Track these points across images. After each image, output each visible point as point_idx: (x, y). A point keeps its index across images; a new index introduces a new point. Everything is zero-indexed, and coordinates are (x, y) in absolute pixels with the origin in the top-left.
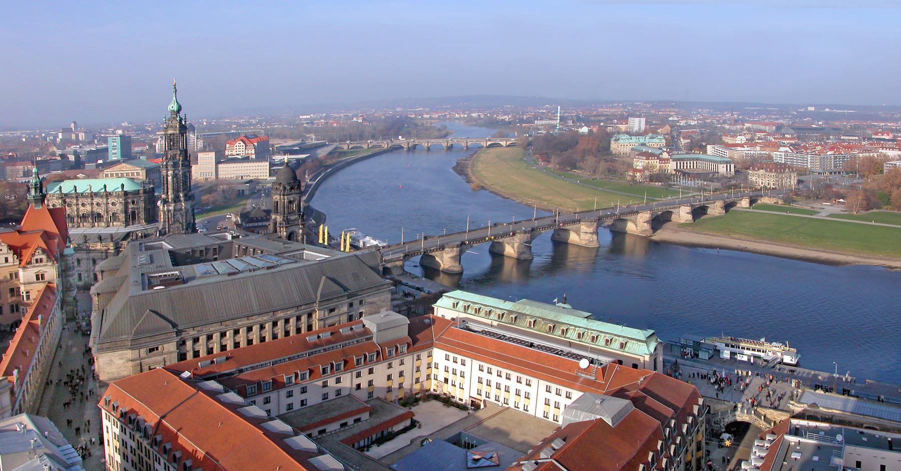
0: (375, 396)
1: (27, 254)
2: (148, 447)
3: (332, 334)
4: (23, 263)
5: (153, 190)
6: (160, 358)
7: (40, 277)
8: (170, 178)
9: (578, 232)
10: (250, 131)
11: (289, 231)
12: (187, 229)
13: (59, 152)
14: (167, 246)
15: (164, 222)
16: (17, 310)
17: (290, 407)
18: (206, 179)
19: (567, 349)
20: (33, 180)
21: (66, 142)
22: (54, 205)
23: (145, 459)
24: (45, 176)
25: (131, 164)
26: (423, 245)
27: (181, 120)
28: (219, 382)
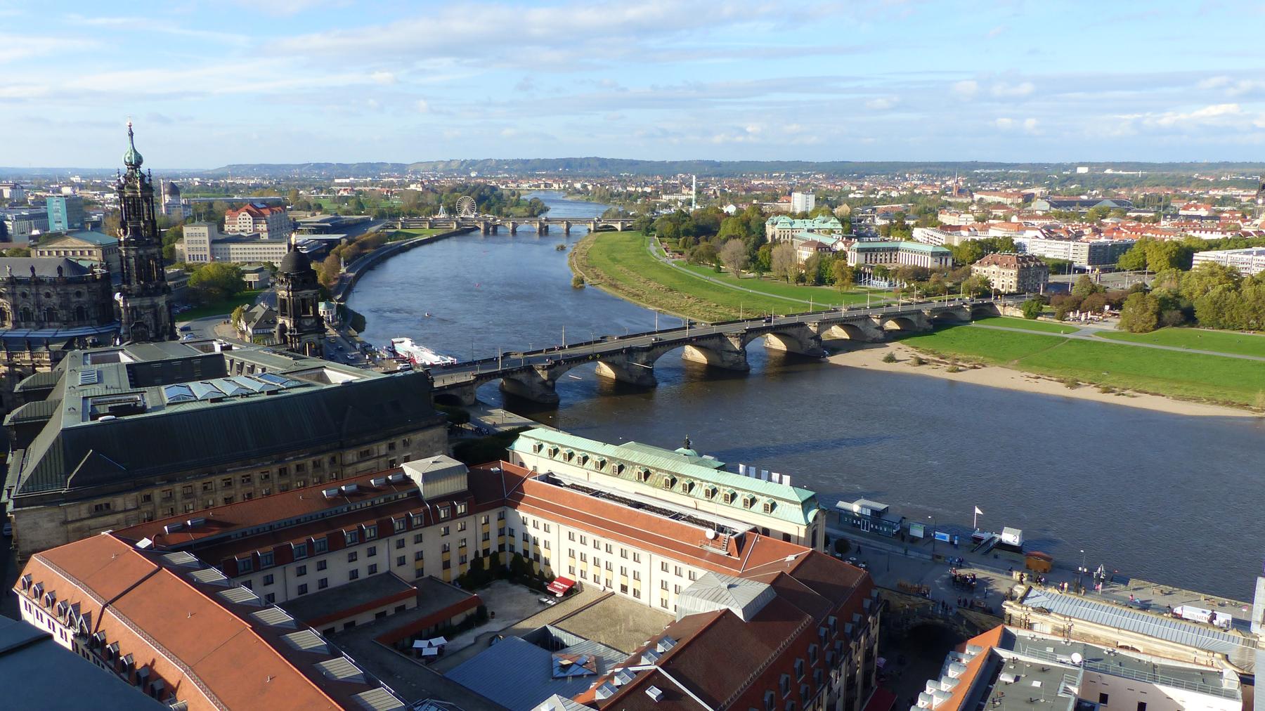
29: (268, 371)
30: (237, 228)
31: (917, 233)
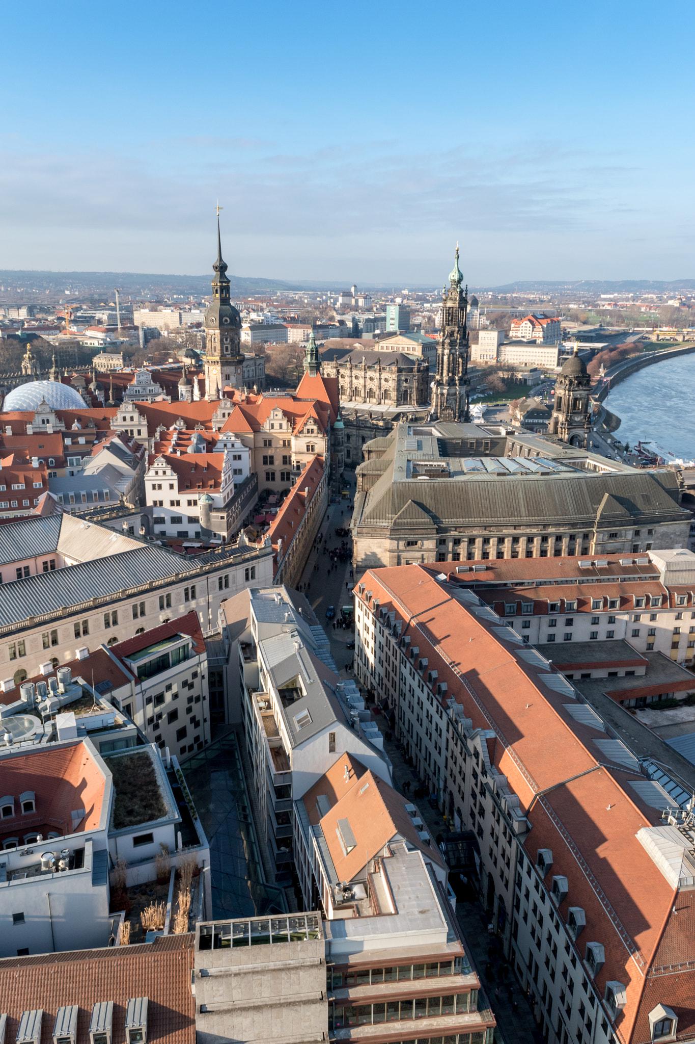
0: (655, 650)
1: (300, 422)
2: (396, 647)
3: (609, 563)
4: (296, 431)
5: (427, 369)
6: (419, 554)
7: (310, 448)
8: (446, 358)
10: (539, 309)
11: (572, 434)
12: (459, 417)
13: (338, 318)
14: (437, 434)
15: (437, 406)
16: (288, 479)
17: (551, 637)
18: (486, 362)
20: (309, 346)
21: (346, 308)
22: (328, 375)
23: (392, 658)
24: (323, 342)
25: (408, 337)
27: (461, 291)
28: (476, 592)
29: (541, 456)
30: (519, 335)
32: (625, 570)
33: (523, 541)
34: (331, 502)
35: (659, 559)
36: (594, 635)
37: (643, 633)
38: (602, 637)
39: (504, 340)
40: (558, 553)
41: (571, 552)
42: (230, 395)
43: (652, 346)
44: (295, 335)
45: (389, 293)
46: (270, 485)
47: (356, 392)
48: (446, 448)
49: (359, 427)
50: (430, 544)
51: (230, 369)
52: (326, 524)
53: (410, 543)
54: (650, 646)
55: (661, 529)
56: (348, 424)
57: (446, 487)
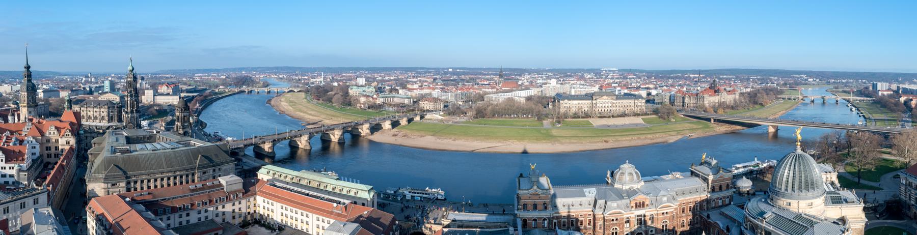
1: (63, 131)
5: (121, 107)
7: (68, 143)
9: (333, 135)
10: (170, 81)
14: (125, 134)
19: (327, 197)
21: (86, 82)
26: (254, 141)
31: (401, 91)
32: (210, 187)
33: (165, 179)
34: (78, 167)
35: (223, 180)
36: (199, 219)
37: (220, 215)
38: (203, 219)
39: (156, 94)
40: (181, 183)
41: (187, 182)
42: (31, 120)
43: (216, 94)
44: (64, 94)
45: (106, 75)
46: (49, 160)
47: (89, 117)
48: (129, 140)
49: (91, 133)
50: (123, 184)
51: (31, 109)
52: (75, 178)
53: (113, 185)
54: (224, 220)
55: (224, 167)
56: (85, 132)
57: (129, 157)
